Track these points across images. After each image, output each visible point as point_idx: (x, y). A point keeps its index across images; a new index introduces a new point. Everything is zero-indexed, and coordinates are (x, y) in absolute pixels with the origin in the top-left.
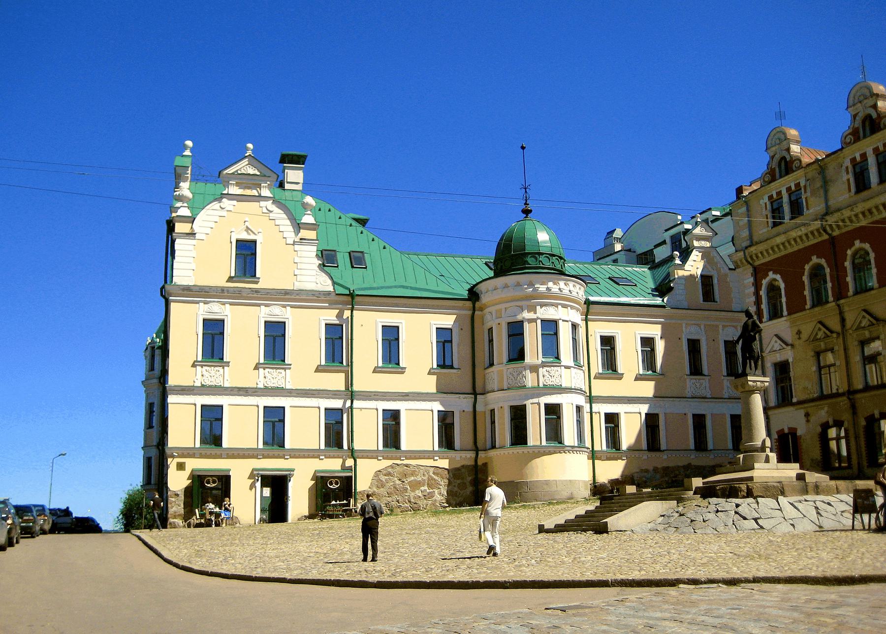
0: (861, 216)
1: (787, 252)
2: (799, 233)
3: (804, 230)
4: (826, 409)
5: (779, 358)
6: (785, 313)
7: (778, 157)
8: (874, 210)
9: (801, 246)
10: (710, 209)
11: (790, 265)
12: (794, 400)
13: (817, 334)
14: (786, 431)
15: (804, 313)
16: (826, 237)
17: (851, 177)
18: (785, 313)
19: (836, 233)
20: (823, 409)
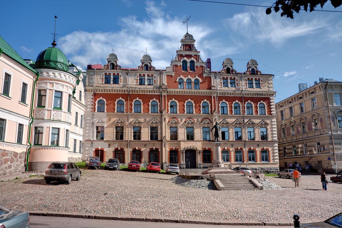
0: (141, 91)
1: (109, 93)
2: (118, 89)
3: (120, 89)
4: (117, 144)
5: (100, 125)
6: (106, 111)
7: (111, 62)
8: (146, 91)
9: (116, 93)
10: (30, 60)
11: (111, 97)
12: (105, 139)
13: (118, 121)
14: (100, 149)
15: (114, 113)
16: (126, 93)
17: (138, 79)
18: (106, 111)
19: (131, 93)
20: (116, 144)
